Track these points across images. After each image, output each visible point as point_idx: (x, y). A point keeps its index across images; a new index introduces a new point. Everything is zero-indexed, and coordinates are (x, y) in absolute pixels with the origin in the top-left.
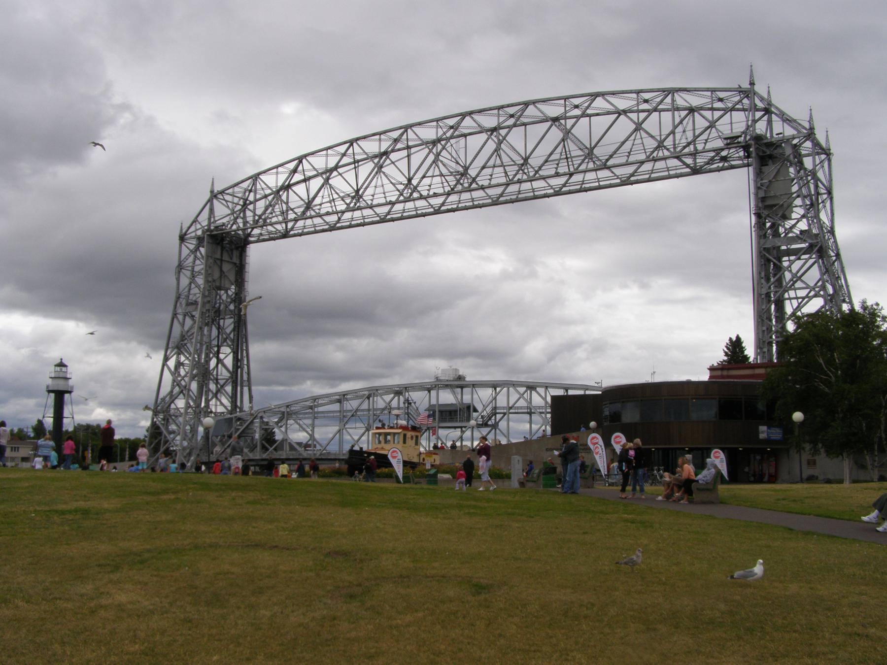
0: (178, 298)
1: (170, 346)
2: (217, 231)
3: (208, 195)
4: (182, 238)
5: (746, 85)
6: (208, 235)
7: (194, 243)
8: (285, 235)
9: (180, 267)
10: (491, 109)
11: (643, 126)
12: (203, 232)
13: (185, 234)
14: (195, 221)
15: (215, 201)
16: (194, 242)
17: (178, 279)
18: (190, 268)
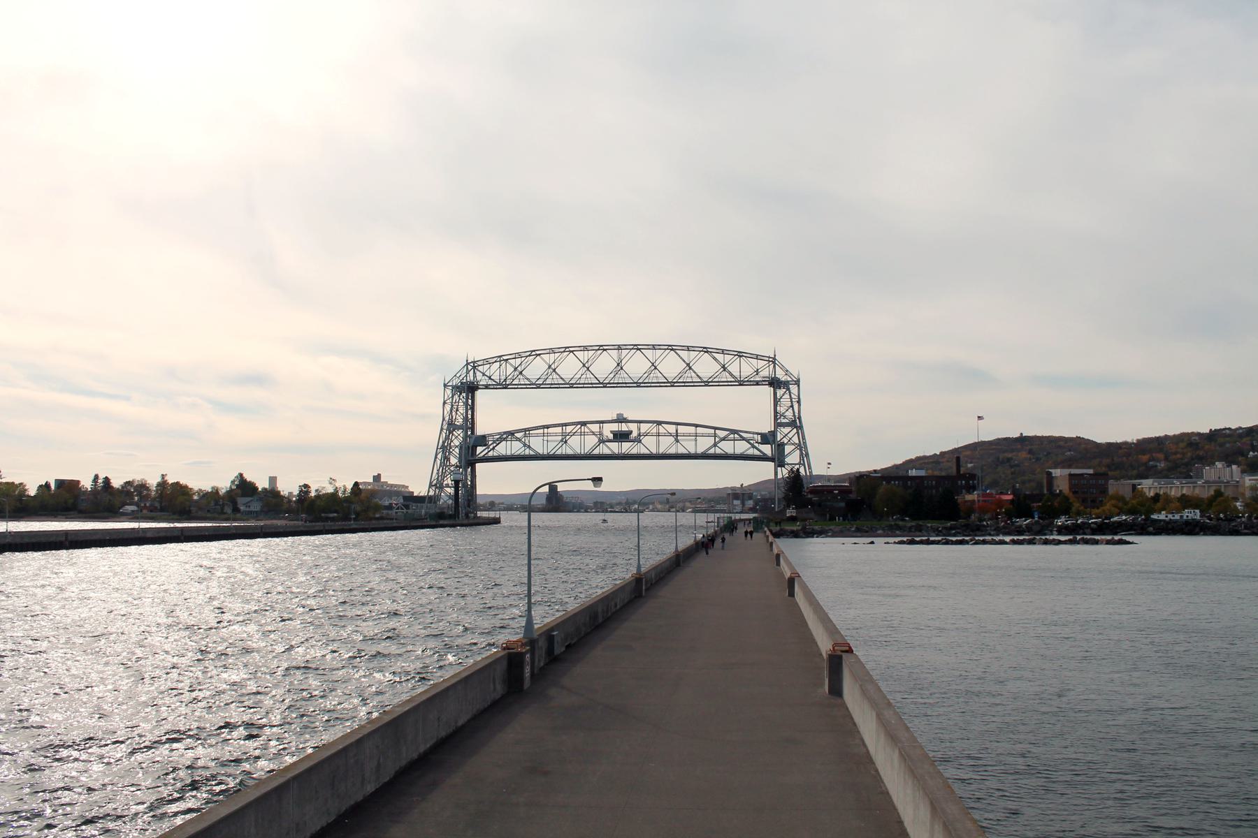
0: (444, 419)
4: (445, 386)
5: (773, 356)
9: (445, 403)
16: (451, 388)
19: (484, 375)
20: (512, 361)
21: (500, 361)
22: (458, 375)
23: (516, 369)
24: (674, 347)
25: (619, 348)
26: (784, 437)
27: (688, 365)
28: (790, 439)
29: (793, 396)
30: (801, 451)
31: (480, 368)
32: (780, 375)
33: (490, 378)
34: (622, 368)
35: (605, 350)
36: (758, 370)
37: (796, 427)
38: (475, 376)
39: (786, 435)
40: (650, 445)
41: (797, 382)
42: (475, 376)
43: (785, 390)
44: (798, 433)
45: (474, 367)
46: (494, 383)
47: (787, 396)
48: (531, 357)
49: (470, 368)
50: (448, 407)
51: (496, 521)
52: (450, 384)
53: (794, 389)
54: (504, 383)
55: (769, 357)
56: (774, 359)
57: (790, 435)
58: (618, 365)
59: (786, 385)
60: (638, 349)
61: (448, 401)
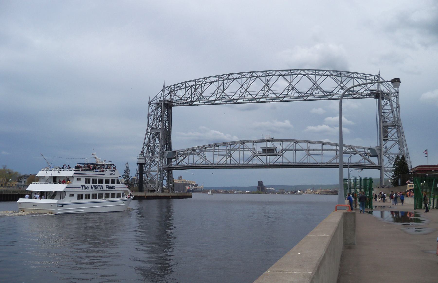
1: (145, 145)
2: (167, 102)
4: (150, 103)
5: (377, 74)
6: (163, 103)
7: (155, 105)
8: (191, 105)
9: (149, 115)
10: (287, 70)
11: (343, 83)
12: (160, 101)
13: (151, 101)
14: (156, 96)
17: (148, 119)
18: (153, 115)
25: (267, 74)
27: (315, 84)
34: (269, 89)
40: (289, 158)
51: (190, 197)
55: (375, 76)
56: (379, 76)
58: (266, 85)
60: (281, 75)
61: (153, 113)
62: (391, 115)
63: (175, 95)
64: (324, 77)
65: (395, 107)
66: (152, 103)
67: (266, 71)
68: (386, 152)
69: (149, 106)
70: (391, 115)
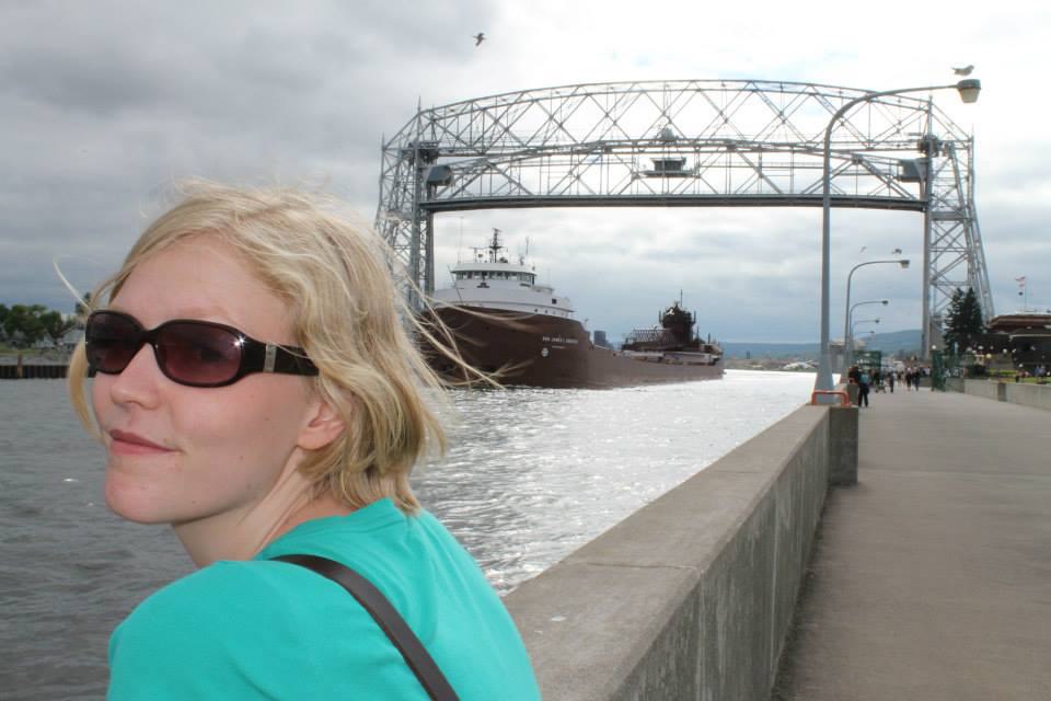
0: (381, 203)
3: (416, 112)
4: (384, 149)
9: (383, 176)
13: (389, 144)
14: (400, 133)
15: (422, 118)
16: (396, 153)
19: (445, 131)
20: (492, 111)
21: (472, 111)
22: (406, 132)
23: (496, 121)
24: (760, 86)
26: (942, 237)
28: (954, 240)
29: (961, 167)
30: (971, 260)
31: (441, 122)
32: (940, 132)
33: (458, 138)
34: (670, 122)
35: (643, 92)
36: (900, 123)
37: (961, 220)
38: (434, 133)
39: (947, 233)
41: (969, 144)
42: (434, 133)
43: (945, 158)
44: (966, 230)
45: (433, 121)
46: (463, 145)
47: (949, 167)
48: (522, 105)
49: (425, 121)
50: (389, 184)
52: (396, 145)
53: (961, 155)
54: (479, 145)
57: (954, 234)
59: (949, 150)
60: (699, 90)
61: (390, 173)
62: (955, 192)
63: (445, 131)
64: (803, 97)
65: (963, 174)
66: (390, 149)
67: (665, 81)
68: (935, 278)
69: (383, 156)
70: (955, 192)
